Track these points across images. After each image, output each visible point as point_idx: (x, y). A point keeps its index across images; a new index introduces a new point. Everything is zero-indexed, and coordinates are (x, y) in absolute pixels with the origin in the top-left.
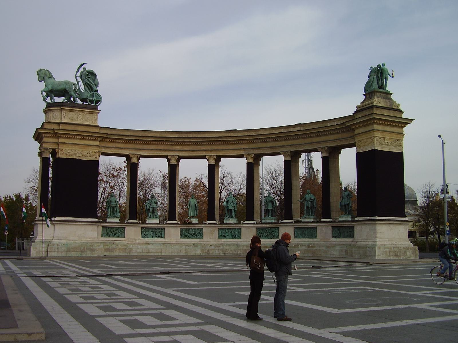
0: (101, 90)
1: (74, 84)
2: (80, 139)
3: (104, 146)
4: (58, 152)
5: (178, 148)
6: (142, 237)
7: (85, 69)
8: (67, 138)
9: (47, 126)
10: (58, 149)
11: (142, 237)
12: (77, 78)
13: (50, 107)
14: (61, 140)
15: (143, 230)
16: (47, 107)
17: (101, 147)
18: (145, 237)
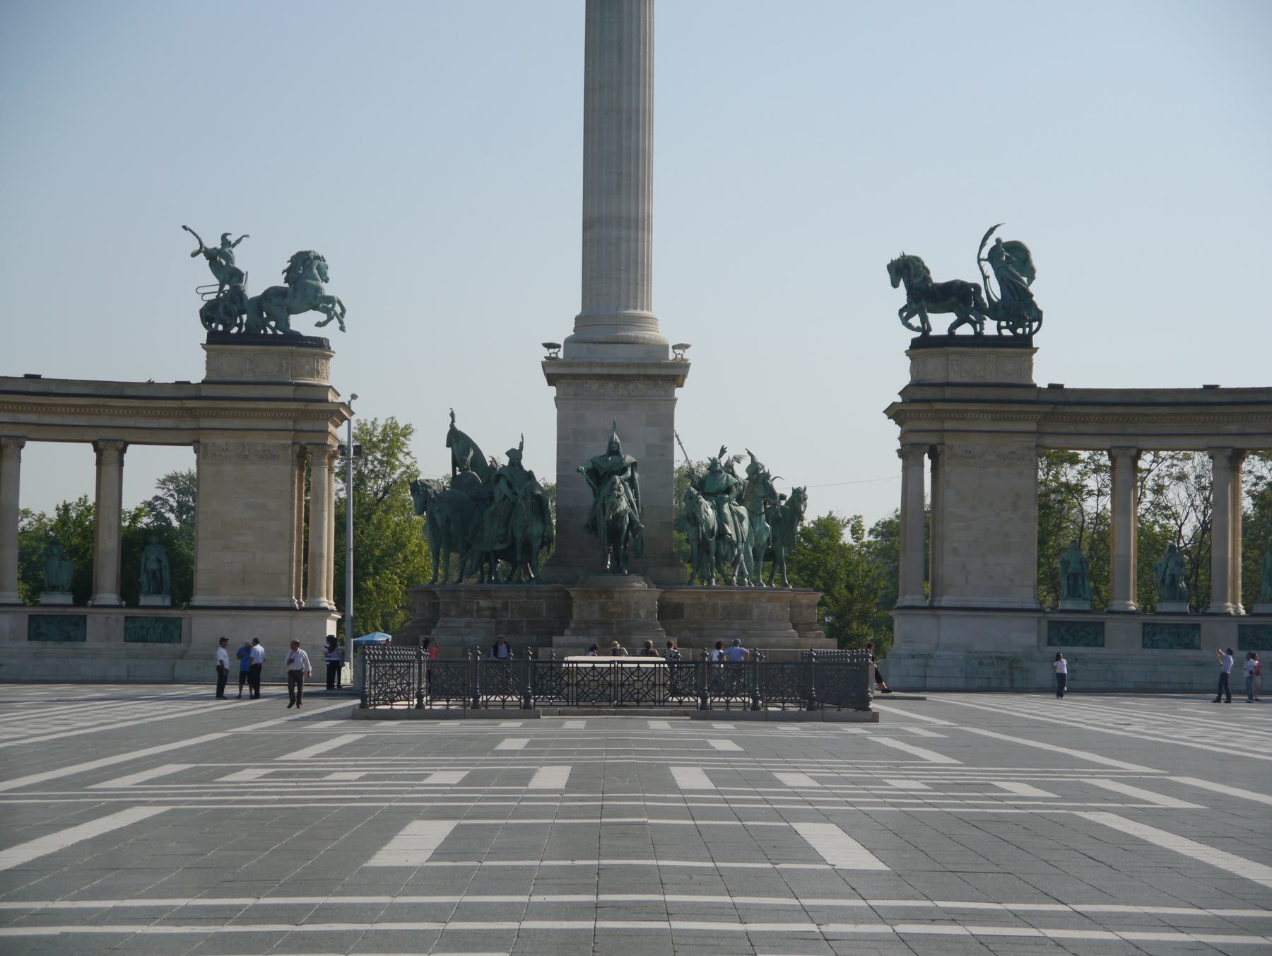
0: (1039, 291)
1: (977, 287)
2: (993, 420)
3: (1050, 430)
4: (943, 451)
5: (1233, 428)
6: (1144, 646)
7: (998, 241)
8: (963, 419)
9: (919, 394)
10: (942, 444)
11: (1144, 646)
12: (983, 263)
13: (923, 345)
14: (949, 425)
15: (1148, 629)
16: (915, 344)
17: (1040, 434)
18: (1152, 647)
